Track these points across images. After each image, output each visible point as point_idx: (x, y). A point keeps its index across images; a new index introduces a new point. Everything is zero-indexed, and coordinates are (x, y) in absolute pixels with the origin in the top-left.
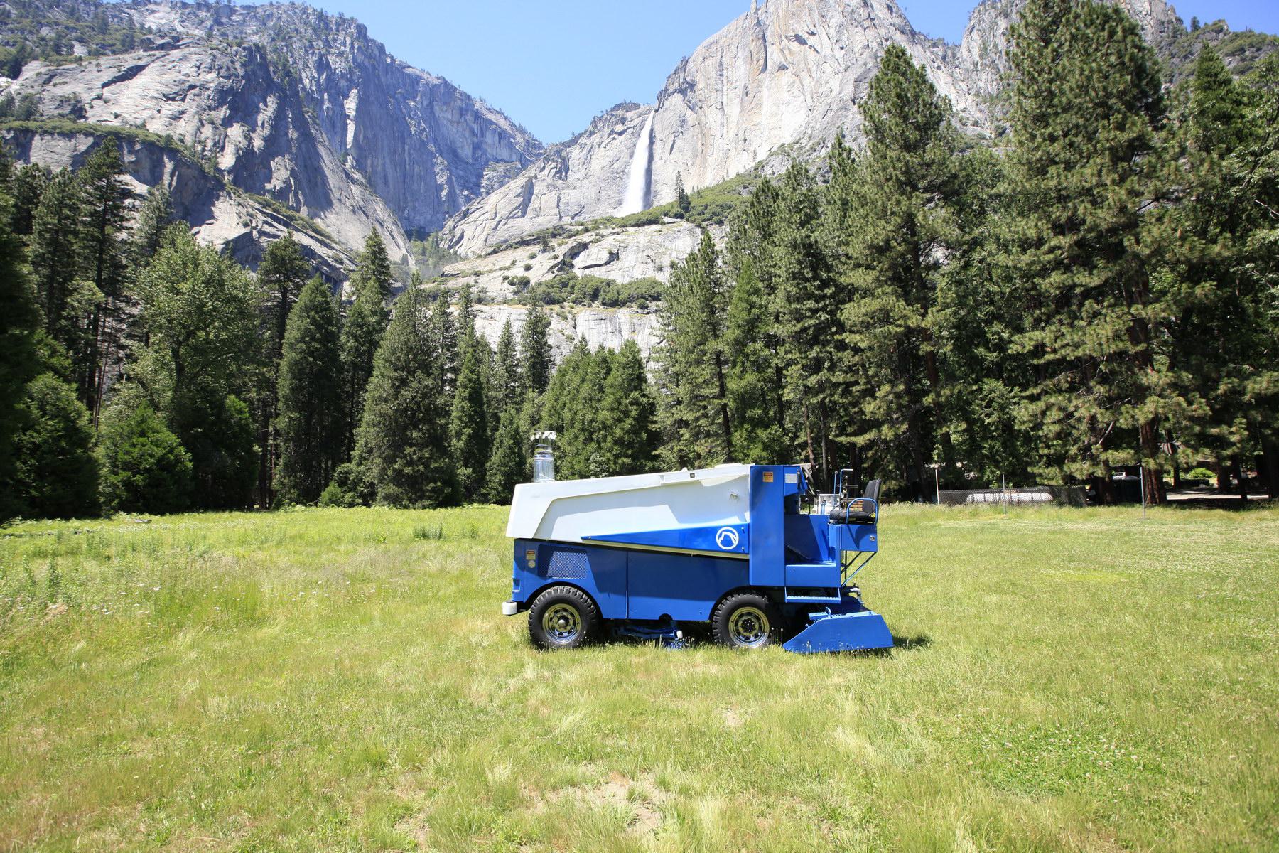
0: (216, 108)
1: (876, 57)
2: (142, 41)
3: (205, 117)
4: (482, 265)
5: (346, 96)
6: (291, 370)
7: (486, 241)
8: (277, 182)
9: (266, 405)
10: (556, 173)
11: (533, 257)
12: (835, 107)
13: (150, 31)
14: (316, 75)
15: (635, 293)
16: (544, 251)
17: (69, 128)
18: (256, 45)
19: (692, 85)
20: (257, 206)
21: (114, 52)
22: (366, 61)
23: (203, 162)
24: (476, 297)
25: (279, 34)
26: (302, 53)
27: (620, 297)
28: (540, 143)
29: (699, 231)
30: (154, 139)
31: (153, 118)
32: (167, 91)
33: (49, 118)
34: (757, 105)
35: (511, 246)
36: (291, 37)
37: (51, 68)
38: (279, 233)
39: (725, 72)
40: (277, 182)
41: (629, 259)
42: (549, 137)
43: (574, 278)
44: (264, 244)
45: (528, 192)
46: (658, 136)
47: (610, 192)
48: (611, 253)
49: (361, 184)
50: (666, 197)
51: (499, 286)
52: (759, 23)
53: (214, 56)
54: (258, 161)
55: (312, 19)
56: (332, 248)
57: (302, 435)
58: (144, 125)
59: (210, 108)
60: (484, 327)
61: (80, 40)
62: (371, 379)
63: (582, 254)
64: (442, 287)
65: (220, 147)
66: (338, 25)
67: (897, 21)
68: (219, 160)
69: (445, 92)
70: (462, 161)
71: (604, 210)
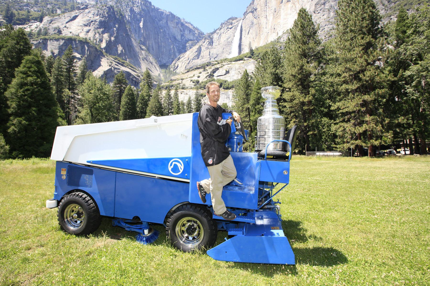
0: (100, 28)
2: (77, 7)
3: (96, 31)
4: (184, 76)
5: (140, 21)
6: (123, 112)
7: (186, 67)
8: (119, 52)
10: (209, 43)
11: (200, 73)
13: (79, 3)
14: (130, 14)
16: (204, 71)
17: (57, 37)
18: (111, 6)
20: (113, 59)
21: (69, 11)
22: (146, 9)
23: (96, 46)
24: (182, 87)
26: (125, 7)
27: (229, 86)
28: (203, 33)
30: (82, 39)
31: (81, 32)
32: (85, 23)
33: (52, 35)
36: (121, 2)
37: (51, 18)
38: (120, 68)
40: (119, 52)
42: (206, 30)
44: (116, 71)
45: (199, 51)
47: (227, 49)
48: (226, 71)
53: (98, 11)
54: (113, 44)
56: (136, 72)
58: (78, 35)
59: (98, 28)
60: (184, 97)
61: (59, 8)
63: (217, 72)
64: (171, 84)
65: (101, 41)
68: (101, 45)
69: (172, 17)
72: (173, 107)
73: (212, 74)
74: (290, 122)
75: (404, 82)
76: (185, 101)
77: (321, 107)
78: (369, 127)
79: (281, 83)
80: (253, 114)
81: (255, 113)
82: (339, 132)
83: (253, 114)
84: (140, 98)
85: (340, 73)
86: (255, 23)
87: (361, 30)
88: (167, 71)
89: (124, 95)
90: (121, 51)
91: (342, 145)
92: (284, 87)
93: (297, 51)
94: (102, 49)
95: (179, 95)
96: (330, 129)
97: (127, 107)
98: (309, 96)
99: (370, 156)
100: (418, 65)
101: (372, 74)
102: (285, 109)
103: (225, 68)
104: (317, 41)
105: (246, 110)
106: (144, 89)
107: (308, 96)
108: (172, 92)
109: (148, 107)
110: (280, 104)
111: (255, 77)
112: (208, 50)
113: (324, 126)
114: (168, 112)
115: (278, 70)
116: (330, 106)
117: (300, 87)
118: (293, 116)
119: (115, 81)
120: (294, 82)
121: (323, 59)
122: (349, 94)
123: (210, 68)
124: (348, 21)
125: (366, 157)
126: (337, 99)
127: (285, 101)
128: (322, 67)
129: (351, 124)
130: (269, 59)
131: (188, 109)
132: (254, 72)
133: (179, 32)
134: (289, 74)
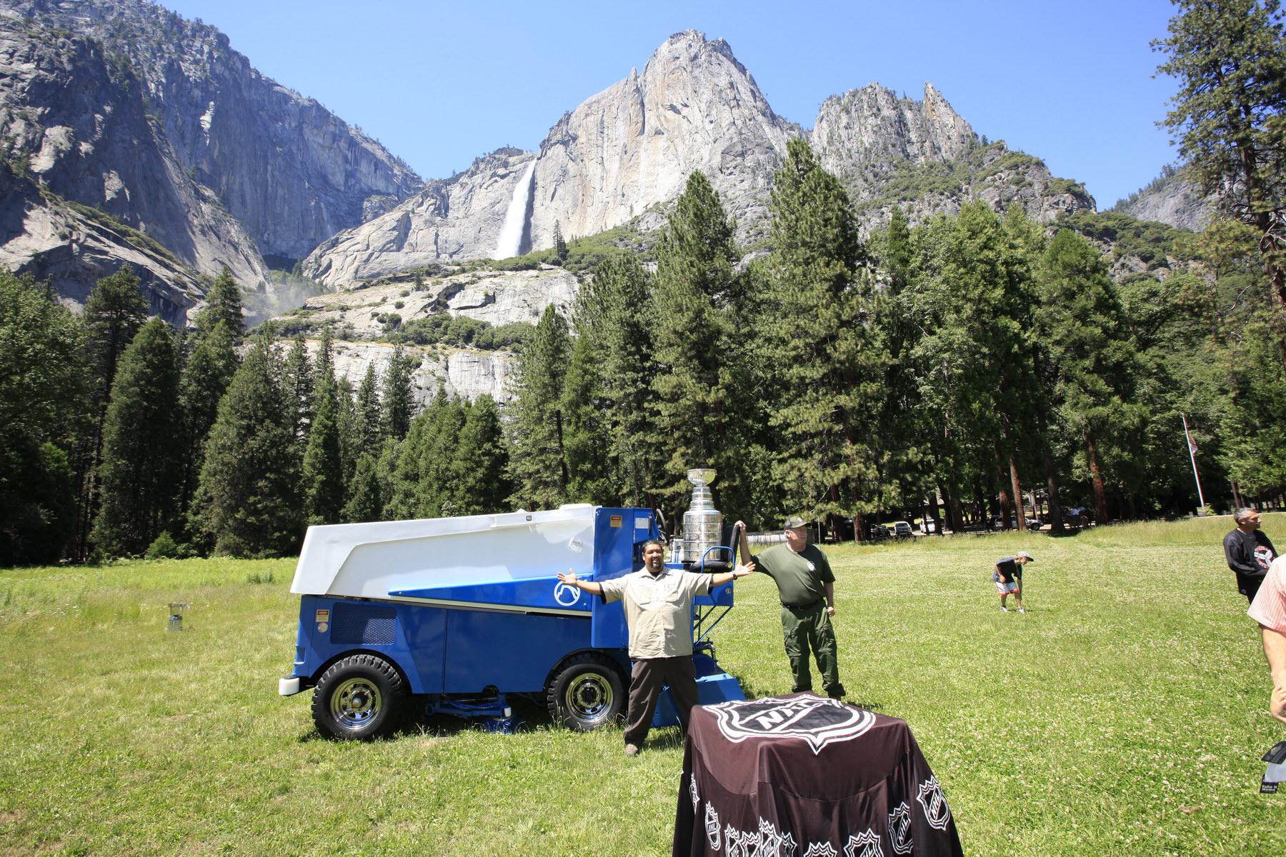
0: (35, 104)
3: (15, 111)
4: (350, 300)
7: (356, 272)
8: (109, 195)
10: (435, 209)
11: (405, 294)
14: (164, 80)
15: (511, 337)
16: (418, 289)
18: (90, 41)
19: (575, 139)
20: (79, 216)
22: (227, 74)
23: (10, 161)
24: (342, 333)
25: (119, 29)
28: (419, 178)
35: (383, 282)
36: (135, 36)
38: (107, 249)
40: (109, 195)
42: (429, 170)
44: (87, 259)
45: (404, 227)
49: (214, 202)
55: (162, 20)
56: (173, 270)
57: (126, 484)
60: (349, 365)
62: (215, 426)
64: (304, 320)
65: (34, 147)
66: (193, 30)
68: (33, 161)
69: (318, 115)
72: (313, 399)
74: (670, 456)
75: (913, 370)
77: (747, 417)
78: (853, 471)
79: (647, 348)
80: (571, 429)
81: (578, 428)
83: (571, 429)
86: (572, 173)
87: (824, 246)
88: (290, 277)
90: (116, 193)
93: (687, 273)
99: (860, 539)
100: (933, 337)
102: (656, 420)
103: (483, 288)
105: (551, 417)
108: (313, 347)
110: (646, 405)
112: (433, 230)
114: (296, 413)
115: (638, 315)
116: (767, 416)
117: (696, 362)
118: (678, 439)
120: (680, 349)
121: (746, 298)
123: (438, 283)
124: (797, 221)
125: (851, 543)
126: (782, 400)
127: (657, 397)
128: (745, 319)
129: (815, 462)
131: (364, 405)
133: (339, 162)
134: (668, 327)
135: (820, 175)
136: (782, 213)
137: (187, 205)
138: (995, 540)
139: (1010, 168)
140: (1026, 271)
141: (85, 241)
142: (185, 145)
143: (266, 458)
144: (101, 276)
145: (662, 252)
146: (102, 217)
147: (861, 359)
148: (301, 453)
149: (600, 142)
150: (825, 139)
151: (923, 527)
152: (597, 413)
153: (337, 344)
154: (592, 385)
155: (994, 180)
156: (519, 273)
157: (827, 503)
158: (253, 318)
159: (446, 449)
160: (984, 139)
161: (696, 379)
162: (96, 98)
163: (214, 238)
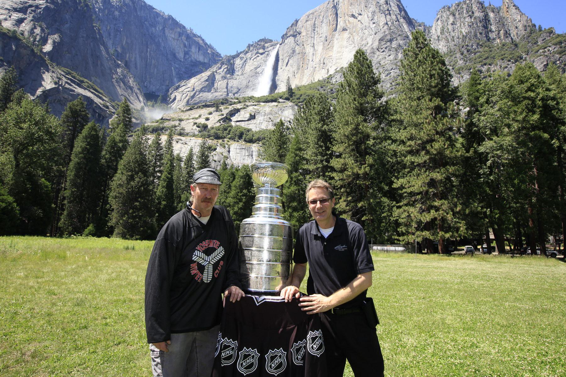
1: (390, 29)
4: (184, 116)
6: (75, 164)
7: (188, 102)
9: (59, 183)
10: (227, 71)
11: (210, 114)
12: (369, 51)
14: (102, 7)
16: (217, 111)
19: (300, 34)
20: (63, 73)
22: (131, 4)
27: (254, 139)
28: (220, 55)
29: (296, 107)
34: (331, 46)
38: (74, 89)
39: (316, 28)
41: (260, 118)
43: (231, 126)
45: (211, 80)
46: (281, 57)
50: (282, 88)
51: (192, 127)
52: (335, 7)
56: (103, 100)
60: (181, 148)
63: (236, 114)
64: (161, 125)
65: (44, 41)
67: (403, 13)
68: (43, 47)
70: (178, 59)
71: (249, 93)
72: (163, 164)
73: (228, 117)
74: (339, 201)
76: (184, 155)
77: (381, 183)
82: (402, 218)
84: (108, 143)
85: (405, 140)
89: (81, 136)
91: (405, 237)
92: (332, 151)
93: (352, 104)
94: (45, 54)
95: (174, 143)
96: (392, 213)
97: (85, 157)
98: (365, 167)
101: (440, 146)
104: (378, 94)
106: (117, 130)
107: (364, 166)
108: (164, 138)
109: (122, 161)
110: (327, 174)
111: (294, 131)
112: (225, 81)
113: (383, 209)
114: (154, 170)
115: (325, 126)
119: (66, 112)
122: (415, 168)
123: (226, 108)
124: (415, 76)
127: (333, 169)
128: (383, 129)
129: (418, 209)
130: (314, 108)
131: (187, 168)
132: (291, 121)
133: (182, 47)
134: (340, 133)
135: (430, 50)
136: (406, 72)
137: (110, 69)
138: (523, 260)
139: (556, 44)
140: (556, 104)
141: (65, 85)
142: (110, 39)
143: (139, 192)
144: (70, 101)
145: (340, 92)
146: (73, 73)
147: (447, 152)
148: (155, 190)
149: (313, 35)
150: (439, 31)
151: (481, 249)
152: (301, 177)
153: (176, 137)
154: (300, 162)
155: (544, 52)
156: (268, 104)
157: (422, 231)
158: (138, 124)
159: (225, 192)
160: (540, 28)
161: (354, 161)
162: (72, 17)
163: (122, 84)
